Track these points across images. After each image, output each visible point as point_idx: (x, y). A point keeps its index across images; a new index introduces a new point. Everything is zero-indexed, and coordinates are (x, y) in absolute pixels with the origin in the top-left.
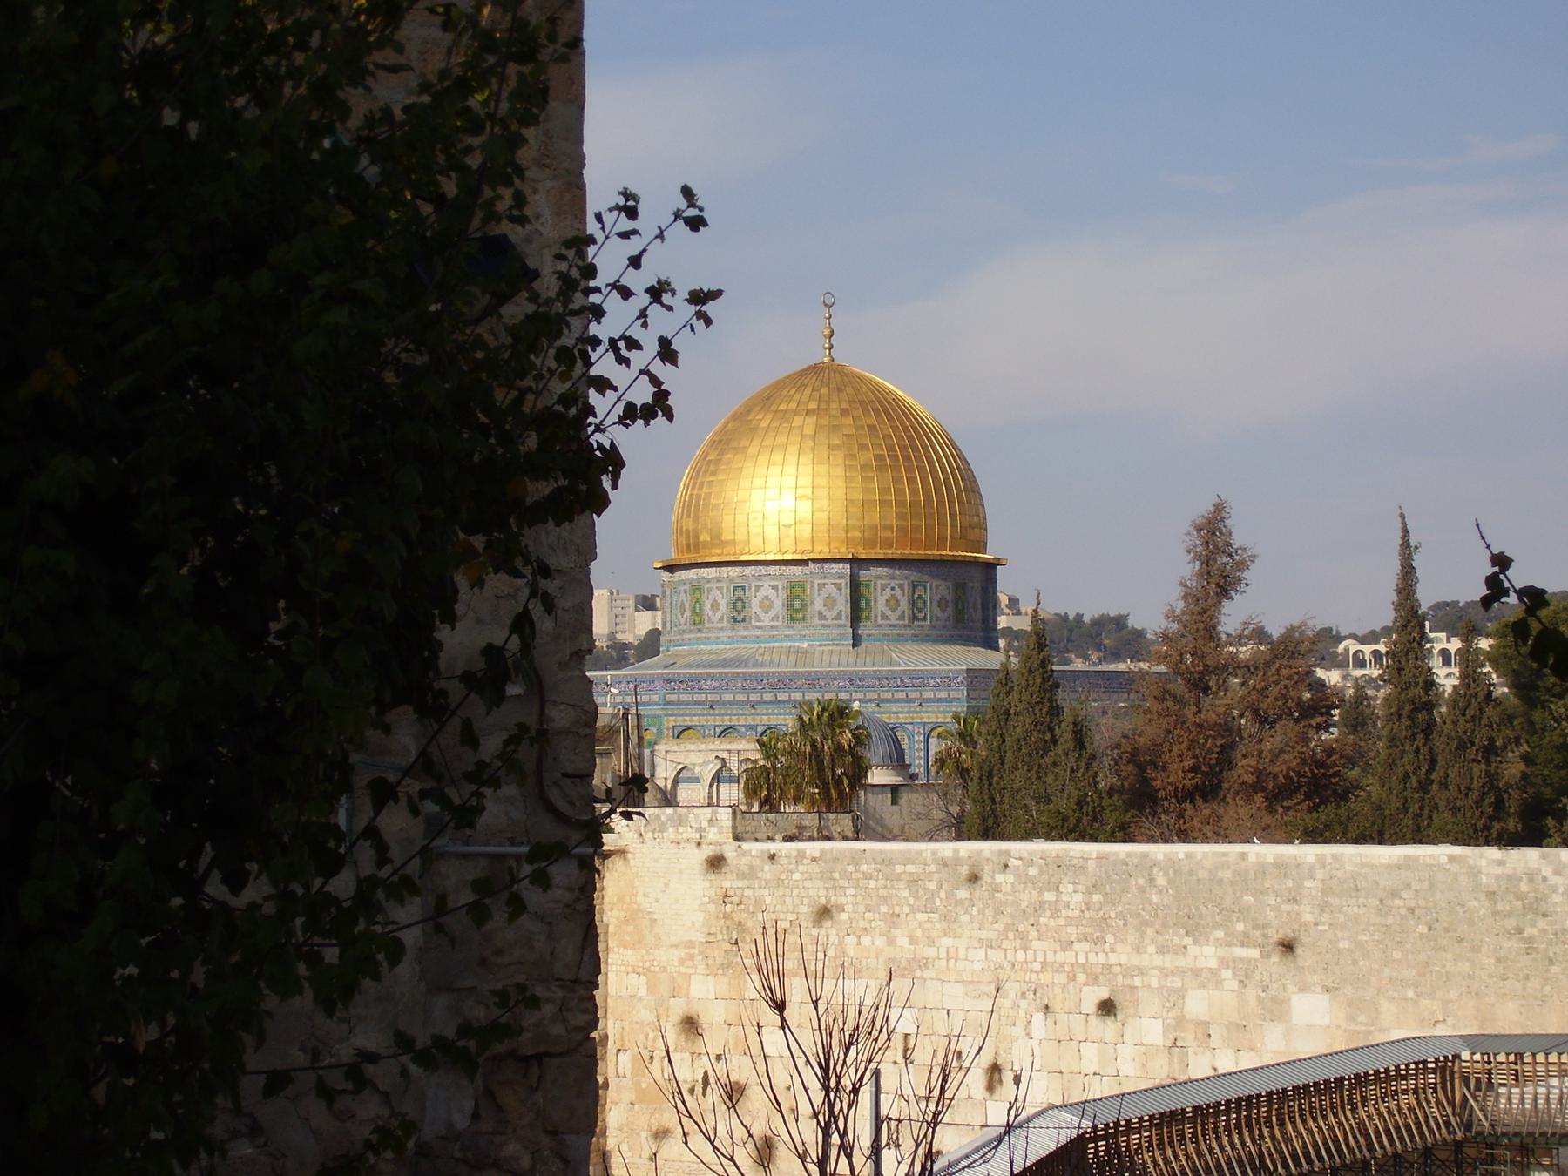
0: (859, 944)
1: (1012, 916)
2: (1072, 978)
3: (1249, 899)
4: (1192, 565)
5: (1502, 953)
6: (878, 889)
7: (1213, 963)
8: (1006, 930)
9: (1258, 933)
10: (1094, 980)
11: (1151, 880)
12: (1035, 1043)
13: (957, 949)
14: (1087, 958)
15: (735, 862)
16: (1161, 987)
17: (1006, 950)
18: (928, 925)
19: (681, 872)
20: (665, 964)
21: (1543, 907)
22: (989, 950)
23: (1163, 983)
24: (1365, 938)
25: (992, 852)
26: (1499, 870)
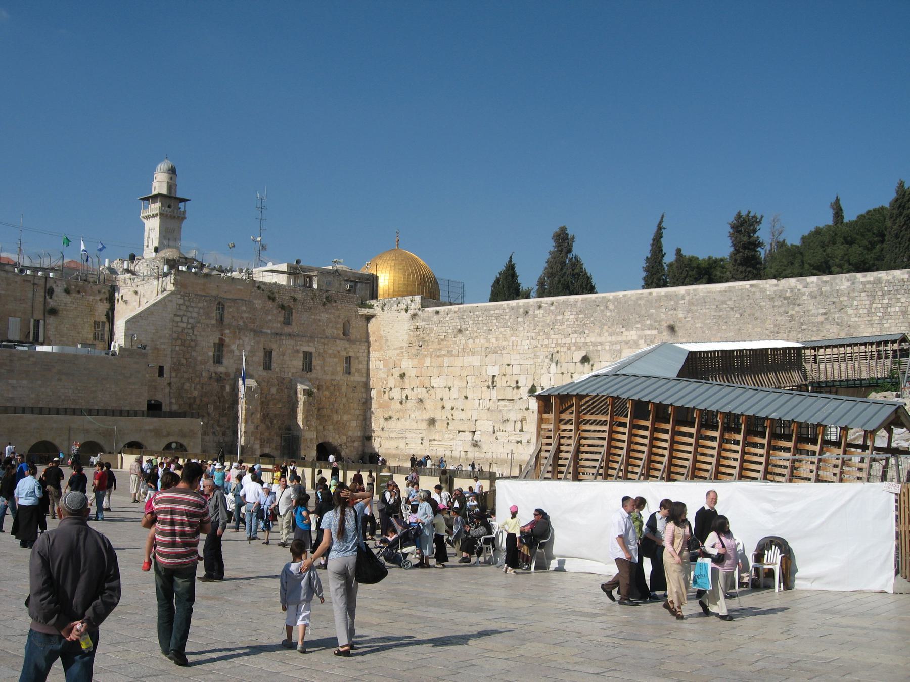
0: (474, 342)
1: (542, 326)
2: (569, 349)
3: (652, 311)
5: (777, 322)
7: (635, 338)
8: (539, 332)
9: (656, 324)
10: (580, 349)
11: (607, 307)
16: (610, 350)
18: (504, 333)
19: (399, 321)
21: (798, 302)
23: (611, 347)
25: (534, 302)
26: (775, 288)
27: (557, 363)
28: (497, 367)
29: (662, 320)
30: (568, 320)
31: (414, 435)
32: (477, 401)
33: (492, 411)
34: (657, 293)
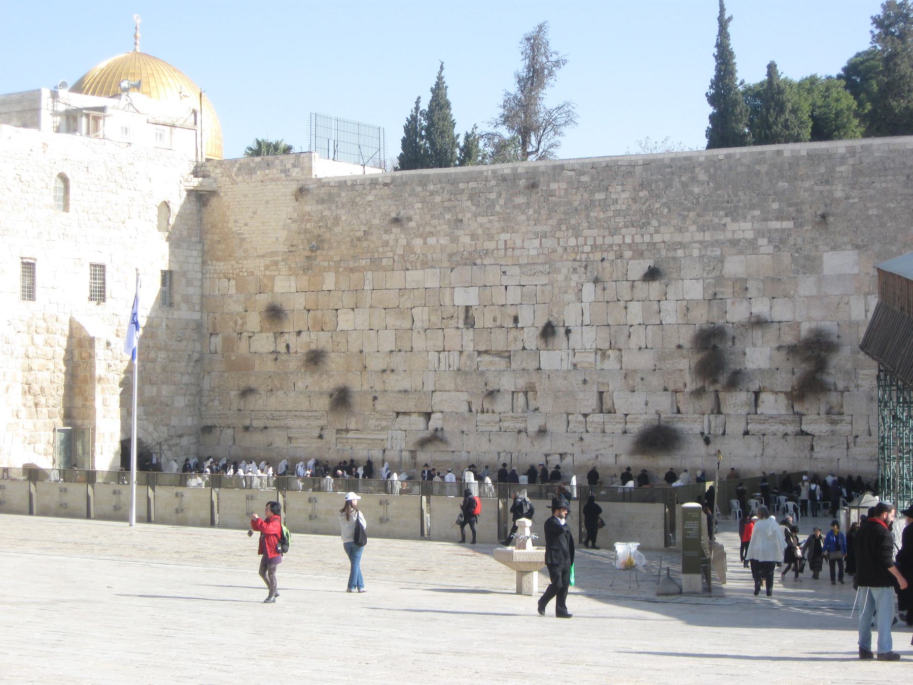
0: (425, 243)
3: (783, 185)
4: (524, 62)
6: (443, 202)
7: (750, 235)
9: (791, 209)
10: (640, 255)
11: (694, 179)
12: (586, 306)
13: (514, 241)
14: (633, 239)
15: (315, 192)
16: (701, 257)
17: (559, 239)
18: (488, 225)
19: (267, 202)
20: (253, 270)
22: (543, 240)
23: (703, 253)
24: (892, 205)
25: (547, 167)
27: (596, 281)
28: (474, 291)
29: (803, 203)
30: (616, 202)
31: (303, 422)
32: (433, 356)
33: (466, 373)
34: (792, 151)
